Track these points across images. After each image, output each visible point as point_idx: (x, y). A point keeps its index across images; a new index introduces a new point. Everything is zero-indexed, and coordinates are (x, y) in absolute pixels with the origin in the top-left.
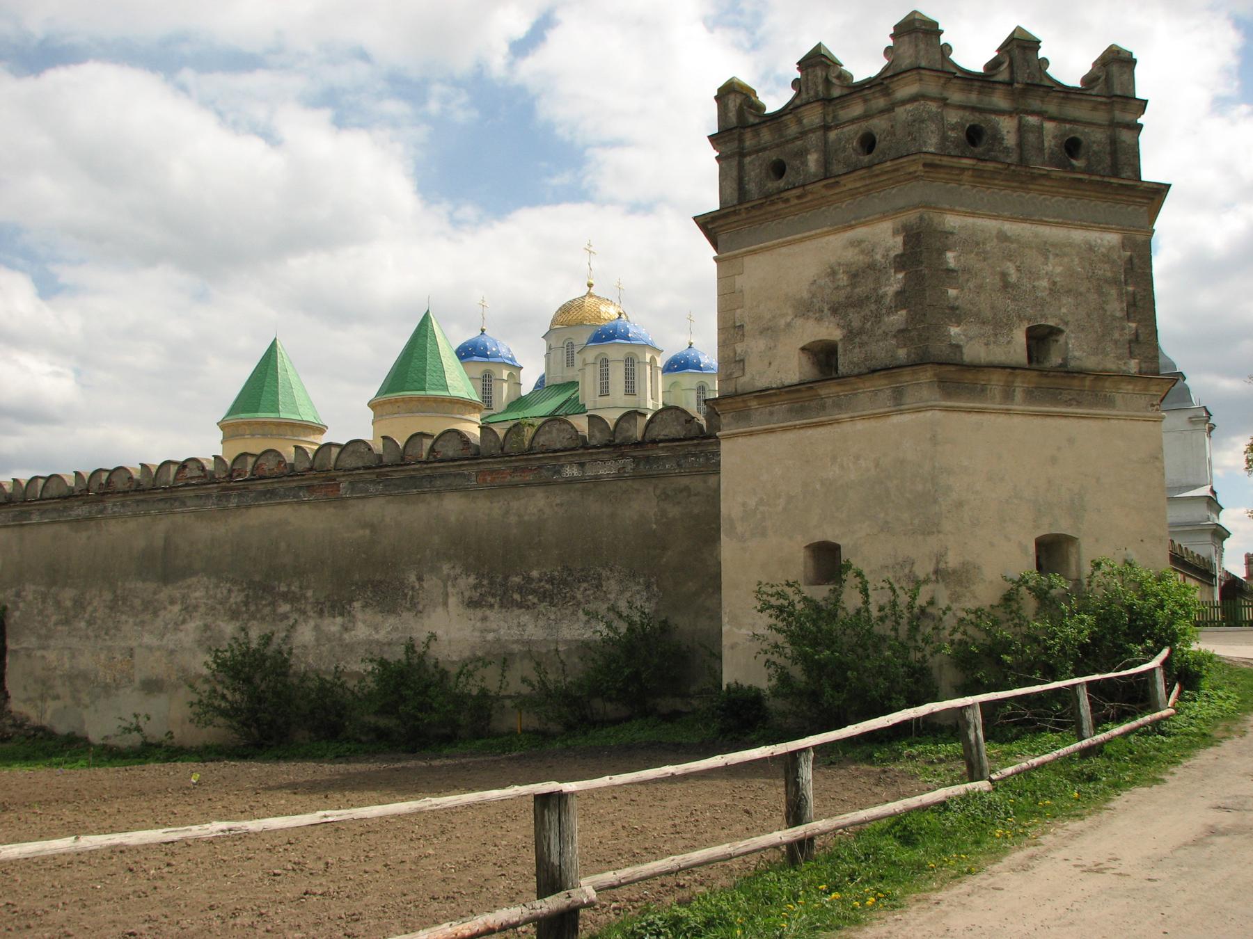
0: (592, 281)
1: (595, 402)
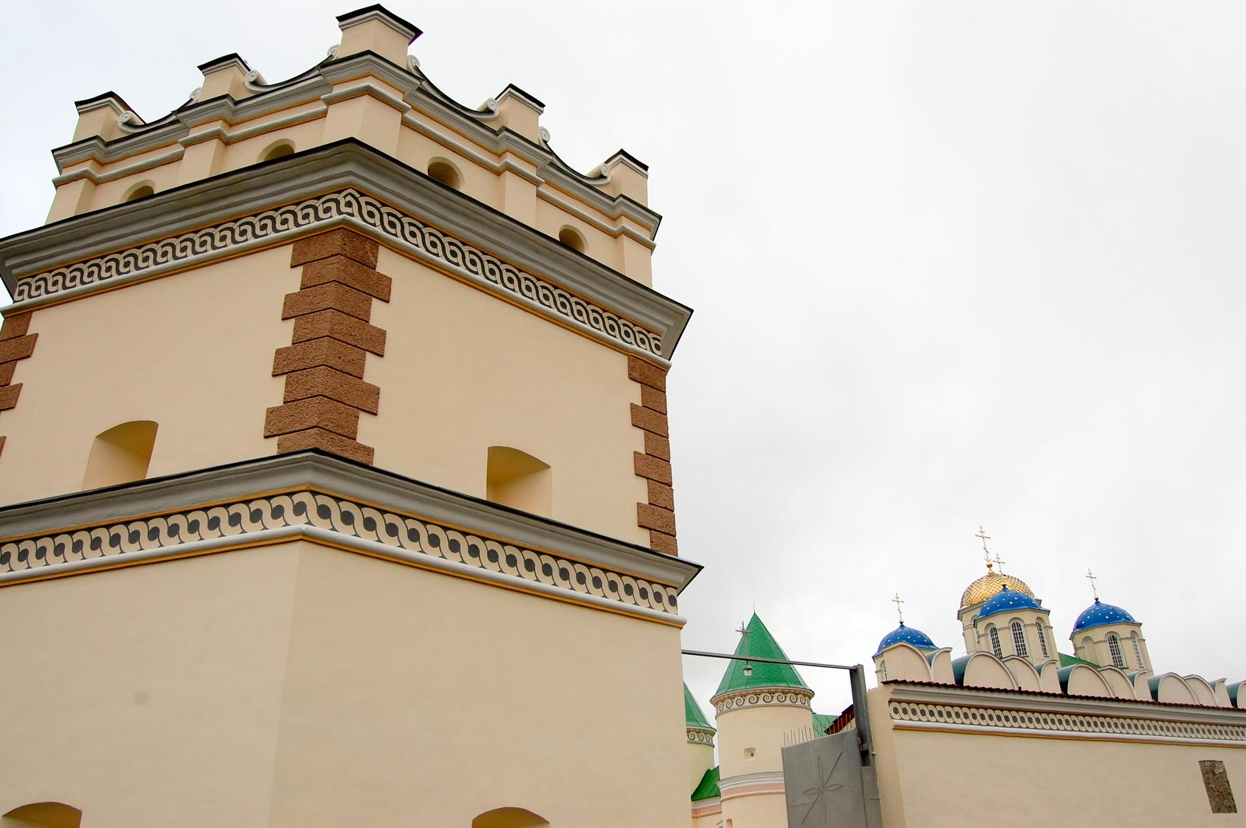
0: (989, 563)
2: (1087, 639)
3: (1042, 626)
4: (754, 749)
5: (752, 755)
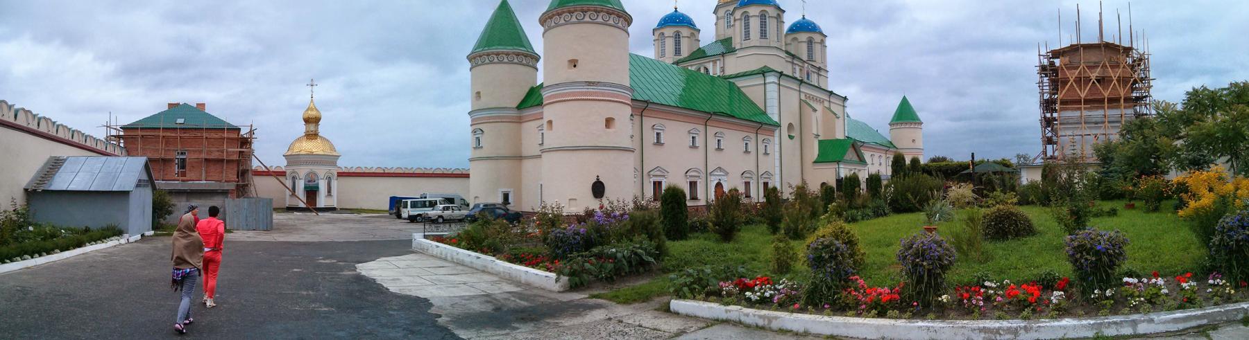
1: (741, 44)
2: (795, 39)
4: (577, 61)
5: (575, 66)
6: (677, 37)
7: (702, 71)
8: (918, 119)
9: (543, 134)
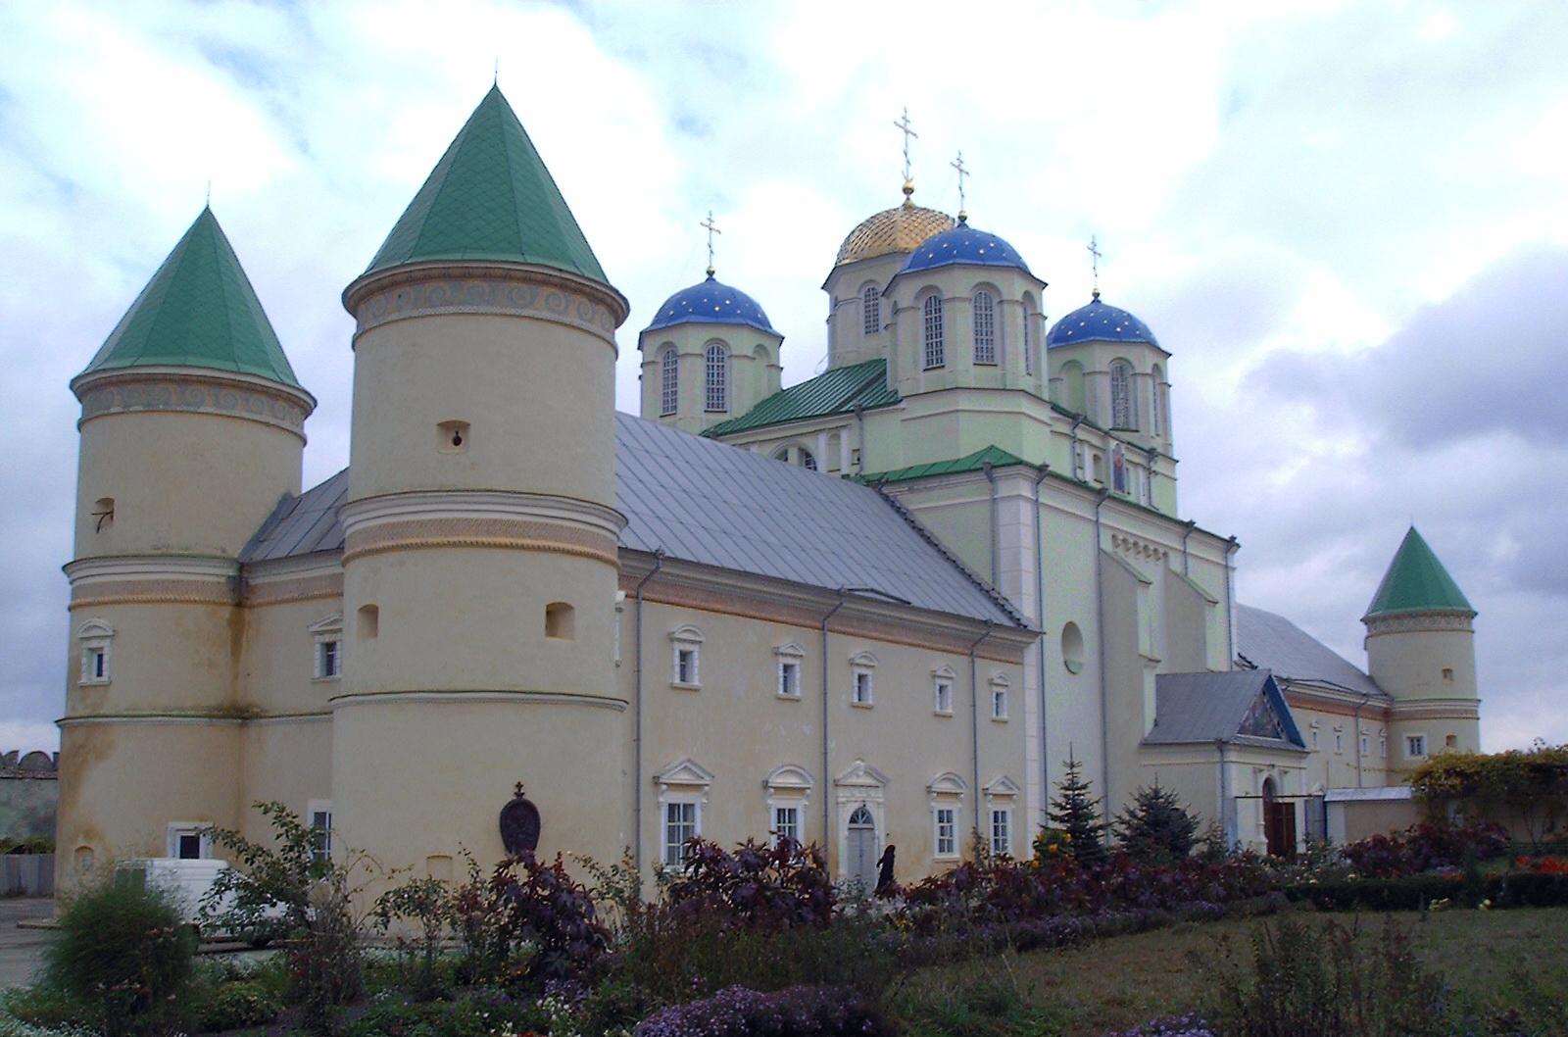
0: (910, 185)
2: (1072, 365)
3: (1029, 312)
4: (465, 426)
5: (457, 441)
6: (716, 355)
7: (793, 455)
8: (1465, 604)
9: (330, 647)
